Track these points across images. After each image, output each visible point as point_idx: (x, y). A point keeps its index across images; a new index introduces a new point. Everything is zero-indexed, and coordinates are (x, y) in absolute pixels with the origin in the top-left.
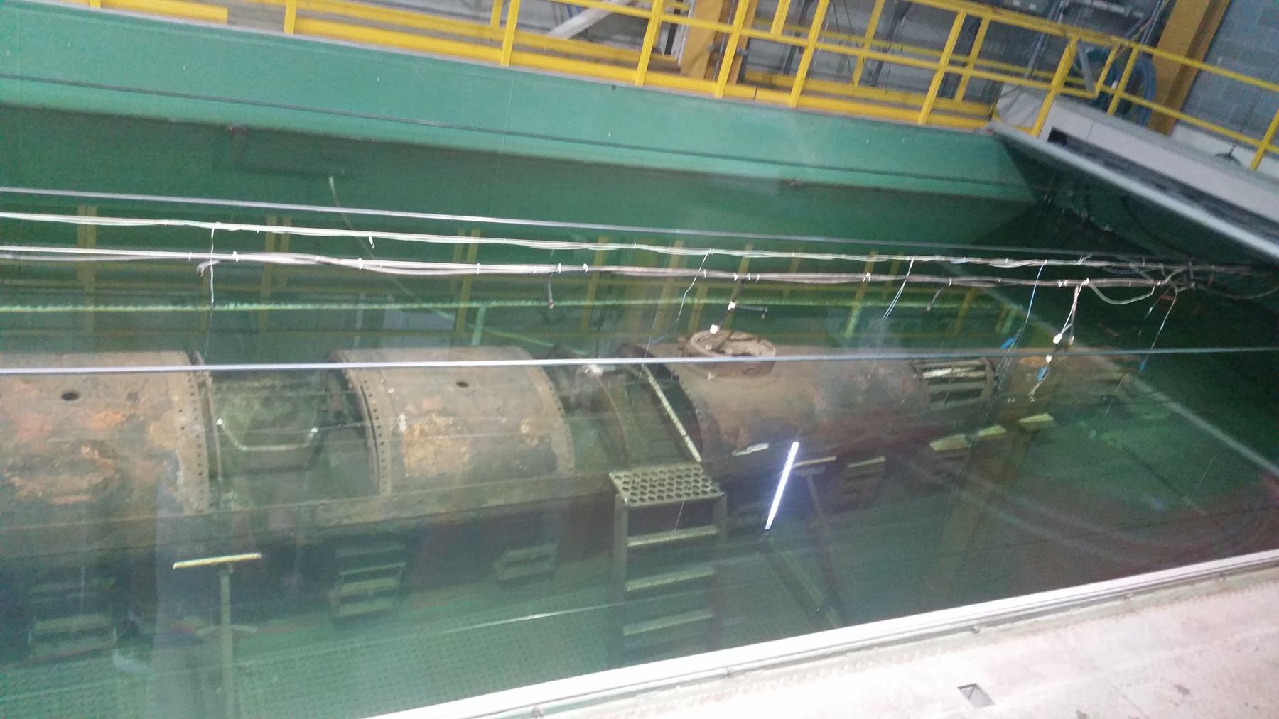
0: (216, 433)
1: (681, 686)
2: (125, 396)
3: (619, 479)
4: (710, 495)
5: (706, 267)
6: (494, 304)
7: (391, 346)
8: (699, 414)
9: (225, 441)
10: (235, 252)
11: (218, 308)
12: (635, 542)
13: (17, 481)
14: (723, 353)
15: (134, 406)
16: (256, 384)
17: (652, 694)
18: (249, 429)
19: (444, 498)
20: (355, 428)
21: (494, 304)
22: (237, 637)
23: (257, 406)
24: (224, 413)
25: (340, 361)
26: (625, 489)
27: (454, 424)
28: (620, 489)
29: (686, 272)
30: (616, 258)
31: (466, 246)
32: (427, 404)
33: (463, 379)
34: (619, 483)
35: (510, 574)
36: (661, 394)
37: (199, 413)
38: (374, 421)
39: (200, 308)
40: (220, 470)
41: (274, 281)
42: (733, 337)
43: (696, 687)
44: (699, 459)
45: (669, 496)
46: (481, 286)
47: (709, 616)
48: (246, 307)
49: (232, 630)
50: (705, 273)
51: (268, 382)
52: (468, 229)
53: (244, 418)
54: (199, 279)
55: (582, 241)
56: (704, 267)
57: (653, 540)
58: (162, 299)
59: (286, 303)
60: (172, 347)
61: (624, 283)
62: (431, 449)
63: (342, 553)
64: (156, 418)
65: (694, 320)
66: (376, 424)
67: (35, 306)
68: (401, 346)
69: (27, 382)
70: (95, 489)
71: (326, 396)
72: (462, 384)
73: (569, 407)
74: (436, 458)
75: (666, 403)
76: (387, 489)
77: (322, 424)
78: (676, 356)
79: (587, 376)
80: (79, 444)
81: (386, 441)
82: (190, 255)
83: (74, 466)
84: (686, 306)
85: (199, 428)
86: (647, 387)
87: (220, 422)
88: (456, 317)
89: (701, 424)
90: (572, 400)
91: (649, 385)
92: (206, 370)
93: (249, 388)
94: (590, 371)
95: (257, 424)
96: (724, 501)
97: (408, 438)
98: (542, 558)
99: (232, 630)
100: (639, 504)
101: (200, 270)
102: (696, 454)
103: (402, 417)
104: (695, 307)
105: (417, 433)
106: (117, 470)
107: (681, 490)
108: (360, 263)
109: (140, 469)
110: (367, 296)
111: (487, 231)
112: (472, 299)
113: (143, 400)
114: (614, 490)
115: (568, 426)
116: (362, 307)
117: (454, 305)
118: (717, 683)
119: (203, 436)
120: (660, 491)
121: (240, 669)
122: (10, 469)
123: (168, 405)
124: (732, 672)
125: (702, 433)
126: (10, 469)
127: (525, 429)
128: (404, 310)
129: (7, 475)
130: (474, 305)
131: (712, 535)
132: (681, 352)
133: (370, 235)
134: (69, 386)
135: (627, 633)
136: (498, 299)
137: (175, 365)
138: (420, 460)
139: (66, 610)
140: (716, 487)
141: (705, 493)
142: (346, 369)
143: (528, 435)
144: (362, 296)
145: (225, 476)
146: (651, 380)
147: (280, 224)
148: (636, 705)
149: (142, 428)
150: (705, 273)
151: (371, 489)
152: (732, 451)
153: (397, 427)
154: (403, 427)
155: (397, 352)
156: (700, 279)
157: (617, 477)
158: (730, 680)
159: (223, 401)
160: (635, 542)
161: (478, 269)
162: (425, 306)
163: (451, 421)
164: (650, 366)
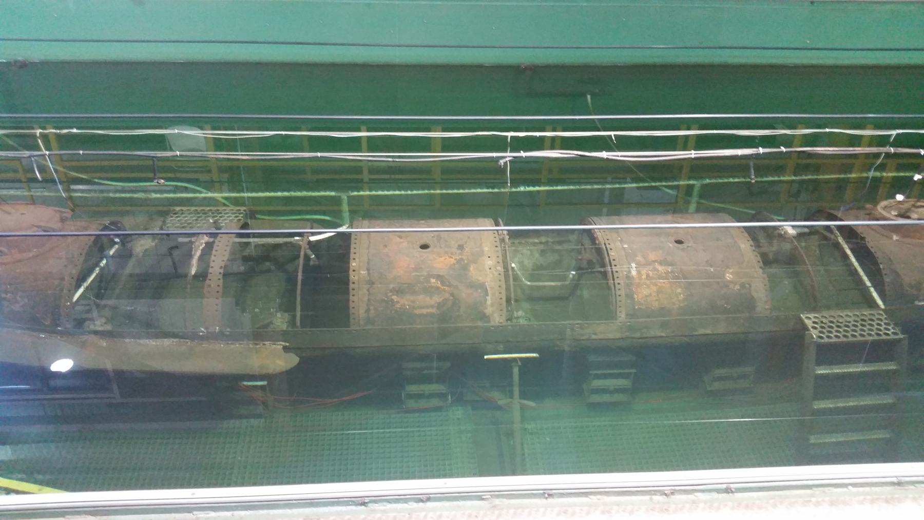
0: (510, 273)
1: (853, 487)
2: (456, 246)
3: (809, 319)
4: (893, 337)
5: (893, 145)
6: (708, 181)
7: (629, 214)
8: (884, 269)
9: (516, 278)
10: (521, 151)
11: (514, 190)
12: (821, 371)
13: (394, 297)
14: (909, 218)
15: (460, 254)
16: (536, 241)
17: (826, 489)
18: (533, 270)
19: (664, 325)
20: (601, 272)
21: (708, 181)
22: (523, 408)
23: (537, 255)
24: (516, 260)
25: (591, 224)
26: (814, 328)
27: (672, 272)
28: (810, 327)
29: (874, 150)
30: (813, 140)
31: (687, 137)
32: (652, 256)
33: (680, 238)
34: (809, 323)
35: (717, 386)
36: (849, 252)
37: (500, 260)
38: (613, 267)
39: (503, 190)
40: (513, 296)
41: (550, 171)
42: (919, 204)
43: (867, 489)
44: (883, 307)
45: (853, 336)
46: (698, 168)
47: (888, 436)
48: (531, 189)
49: (520, 403)
50: (892, 150)
51: (543, 239)
52: (688, 124)
53: (529, 263)
54: (502, 171)
55: (783, 129)
56: (892, 145)
57: (837, 370)
58: (479, 184)
59: (557, 186)
60: (485, 216)
61: (819, 161)
62: (655, 288)
63: (592, 358)
64: (475, 262)
65: (882, 190)
66: (614, 269)
67: (407, 191)
68: (637, 214)
69: (400, 237)
70: (439, 306)
71: (581, 249)
72: (679, 242)
73: (767, 261)
74: (658, 295)
75: (853, 260)
76: (622, 316)
77: (579, 269)
78: (864, 220)
79: (783, 237)
80: (430, 276)
81: (622, 282)
82: (495, 155)
83: (429, 291)
84: (874, 179)
85: (500, 268)
86: (837, 246)
87: (513, 265)
88: (678, 192)
89: (885, 277)
90: (771, 256)
91: (838, 243)
92: (504, 230)
93: (531, 243)
94: (786, 233)
95: (538, 267)
96: (906, 342)
97: (637, 281)
98: (744, 376)
99: (520, 403)
100: (826, 340)
101: (501, 163)
102: (880, 302)
103: (634, 265)
104: (883, 180)
105: (644, 277)
106: (452, 295)
107: (864, 331)
108: (604, 155)
109: (465, 294)
110: (613, 178)
111: (703, 124)
112: (690, 178)
113: (467, 249)
114: (805, 328)
115: (765, 276)
116: (608, 186)
117: (676, 183)
118: (889, 489)
119: (502, 274)
120: (845, 331)
121: (525, 429)
122: (391, 291)
123: (482, 254)
124: (902, 481)
125: (886, 284)
126: (391, 291)
127: (729, 277)
128: (638, 188)
129: (390, 294)
130: (691, 182)
131: (893, 370)
132: (868, 216)
133: (612, 133)
134: (425, 240)
135: (812, 441)
136: (710, 178)
137: (486, 225)
138: (646, 296)
139: (428, 380)
140: (897, 330)
141: (888, 334)
142: (594, 229)
143: (731, 282)
144: (609, 179)
145: (516, 301)
146: (840, 240)
147: (554, 130)
148: (813, 496)
149: (465, 268)
150: (892, 150)
151: (609, 314)
152: (914, 301)
153: (630, 272)
154: (634, 273)
155: (632, 218)
156: (888, 155)
157: (807, 318)
158: (899, 488)
159: (516, 251)
160: (821, 371)
161: (693, 154)
162: (653, 184)
163: (670, 269)
164: (840, 228)
